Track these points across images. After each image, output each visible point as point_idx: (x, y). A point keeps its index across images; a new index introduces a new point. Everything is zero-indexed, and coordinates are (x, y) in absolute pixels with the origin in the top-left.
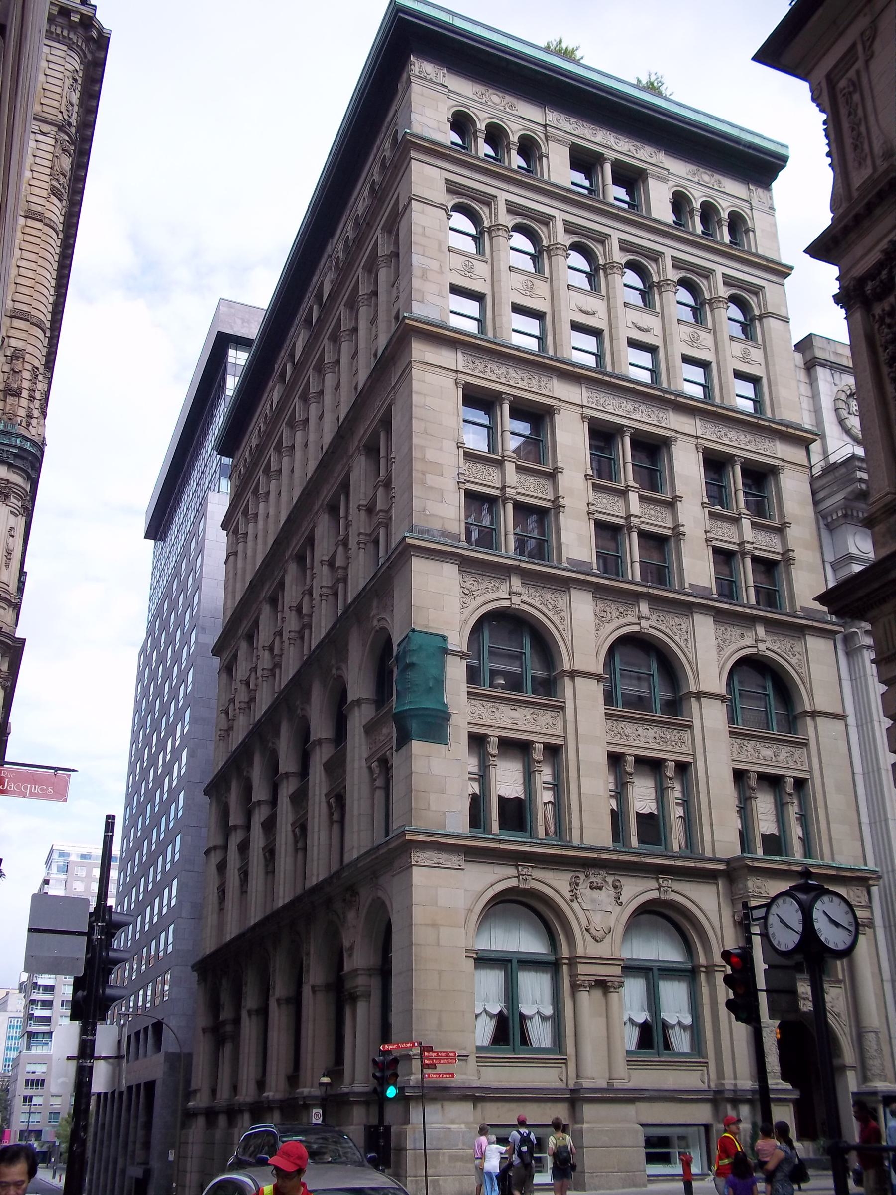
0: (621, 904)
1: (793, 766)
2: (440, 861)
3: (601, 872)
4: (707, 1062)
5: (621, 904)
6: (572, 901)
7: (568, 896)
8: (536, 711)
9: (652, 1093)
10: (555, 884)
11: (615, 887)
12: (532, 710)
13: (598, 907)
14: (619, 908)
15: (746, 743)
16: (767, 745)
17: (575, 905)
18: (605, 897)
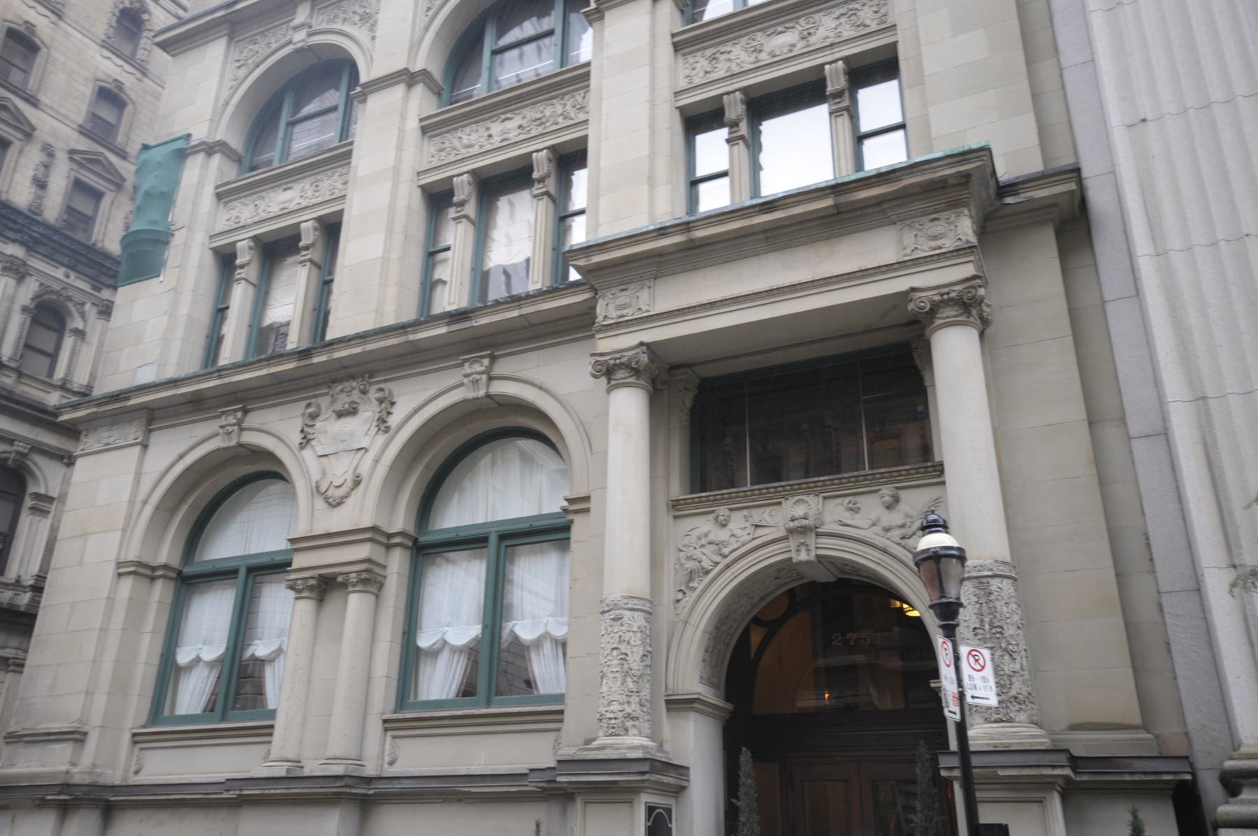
0: (387, 430)
1: (848, 33)
2: (110, 440)
3: (354, 384)
4: (561, 712)
5: (387, 430)
6: (302, 446)
7: (296, 438)
8: (318, 177)
9: (397, 785)
10: (275, 429)
11: (381, 401)
12: (312, 179)
13: (342, 447)
14: (381, 439)
15: (728, 48)
16: (780, 29)
17: (307, 454)
18: (359, 428)
